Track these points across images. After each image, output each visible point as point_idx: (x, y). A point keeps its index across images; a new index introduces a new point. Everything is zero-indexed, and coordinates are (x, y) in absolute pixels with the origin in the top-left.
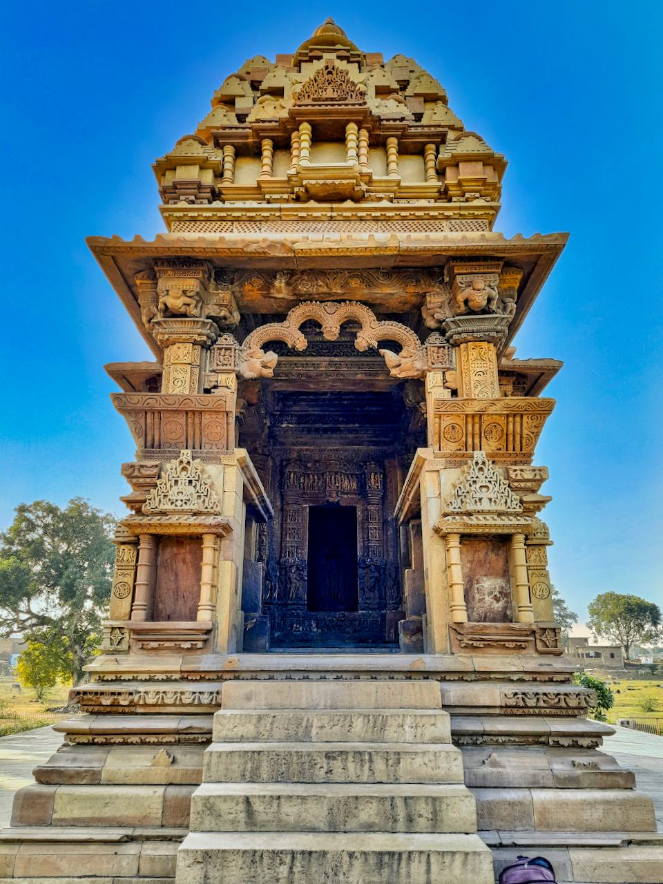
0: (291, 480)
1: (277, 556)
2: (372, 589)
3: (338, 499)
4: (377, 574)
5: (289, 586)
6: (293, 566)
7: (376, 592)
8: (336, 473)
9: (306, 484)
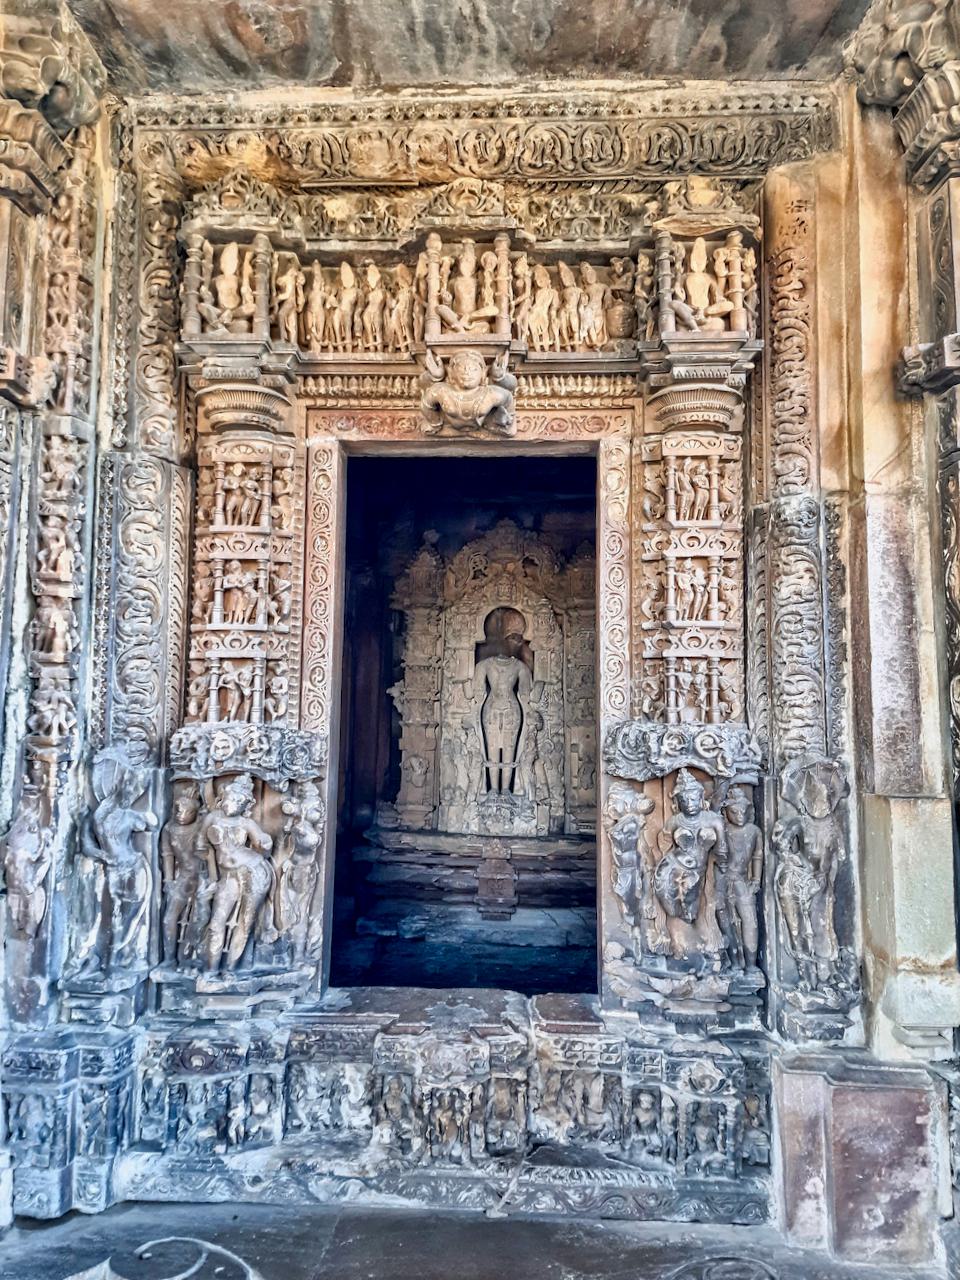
0: (226, 285)
1: (157, 712)
2: (685, 907)
3: (498, 395)
4: (709, 825)
5: (204, 890)
7: (709, 929)
8: (486, 239)
9: (316, 317)
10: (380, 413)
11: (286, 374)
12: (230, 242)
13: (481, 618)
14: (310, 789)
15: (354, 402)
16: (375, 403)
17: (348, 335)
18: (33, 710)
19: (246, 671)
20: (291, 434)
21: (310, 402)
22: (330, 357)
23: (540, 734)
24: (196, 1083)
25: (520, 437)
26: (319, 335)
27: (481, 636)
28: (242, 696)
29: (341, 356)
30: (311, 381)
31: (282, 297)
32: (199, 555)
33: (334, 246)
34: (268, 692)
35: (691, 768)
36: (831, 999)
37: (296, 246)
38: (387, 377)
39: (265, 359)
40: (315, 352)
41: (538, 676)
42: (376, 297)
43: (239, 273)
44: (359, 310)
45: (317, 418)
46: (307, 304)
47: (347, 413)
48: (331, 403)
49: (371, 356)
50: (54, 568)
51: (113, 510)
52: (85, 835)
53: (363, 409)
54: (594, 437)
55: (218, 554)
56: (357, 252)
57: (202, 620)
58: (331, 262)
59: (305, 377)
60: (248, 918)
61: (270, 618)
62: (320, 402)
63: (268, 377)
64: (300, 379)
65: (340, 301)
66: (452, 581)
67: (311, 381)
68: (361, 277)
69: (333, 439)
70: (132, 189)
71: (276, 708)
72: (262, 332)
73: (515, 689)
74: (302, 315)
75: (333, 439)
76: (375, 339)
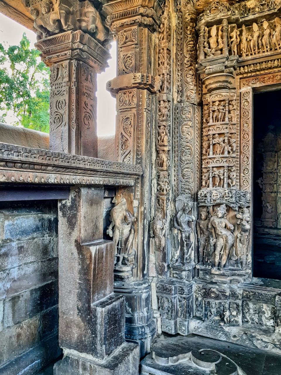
0: (212, 41)
1: (193, 185)
5: (212, 241)
6: (219, 205)
9: (244, 45)
10: (268, 75)
11: (234, 67)
12: (213, 26)
14: (245, 209)
15: (258, 73)
16: (266, 71)
17: (257, 48)
18: (158, 184)
19: (221, 171)
20: (235, 89)
21: (241, 76)
22: (250, 57)
24: (214, 303)
26: (245, 51)
28: (220, 179)
29: (254, 56)
30: (242, 68)
31: (232, 40)
32: (204, 134)
33: (251, 17)
34: (229, 178)
37: (237, 20)
38: (271, 61)
39: (227, 63)
40: (244, 57)
42: (267, 32)
43: (217, 35)
44: (260, 38)
45: (244, 81)
46: (241, 41)
47: (255, 77)
48: (249, 75)
49: (266, 53)
50: (163, 142)
51: (178, 121)
52: (175, 222)
53: (261, 75)
55: (211, 133)
56: (259, 17)
57: (206, 155)
58: (249, 24)
59: (240, 67)
60: (227, 252)
61: (229, 152)
62: (245, 75)
63: (227, 69)
64: (238, 68)
65: (253, 37)
67: (242, 68)
68: (261, 27)
69: (250, 88)
70: (181, 18)
71: (232, 183)
72: (226, 53)
74: (239, 46)
75: (250, 88)
76: (267, 47)
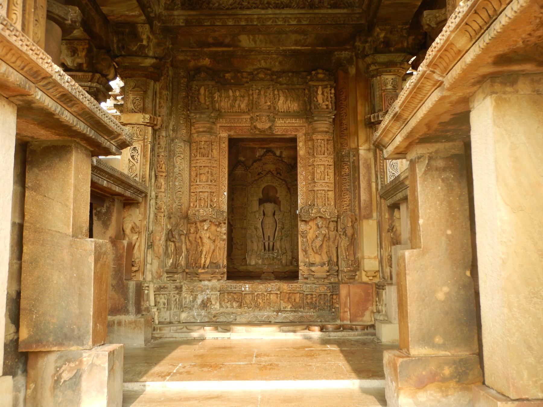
13: (261, 189)
14: (222, 224)
18: (156, 203)
19: (206, 194)
23: (283, 231)
25: (276, 133)
27: (261, 196)
28: (205, 201)
32: (193, 165)
34: (211, 201)
35: (320, 217)
36: (352, 269)
41: (282, 209)
50: (161, 168)
54: (296, 133)
55: (198, 165)
57: (193, 182)
60: (210, 255)
61: (211, 181)
66: (250, 176)
71: (213, 205)
73: (274, 214)
